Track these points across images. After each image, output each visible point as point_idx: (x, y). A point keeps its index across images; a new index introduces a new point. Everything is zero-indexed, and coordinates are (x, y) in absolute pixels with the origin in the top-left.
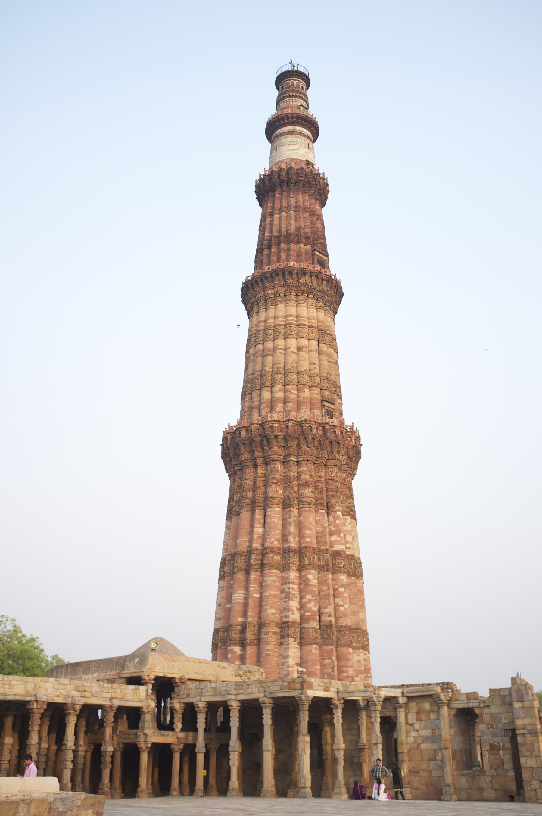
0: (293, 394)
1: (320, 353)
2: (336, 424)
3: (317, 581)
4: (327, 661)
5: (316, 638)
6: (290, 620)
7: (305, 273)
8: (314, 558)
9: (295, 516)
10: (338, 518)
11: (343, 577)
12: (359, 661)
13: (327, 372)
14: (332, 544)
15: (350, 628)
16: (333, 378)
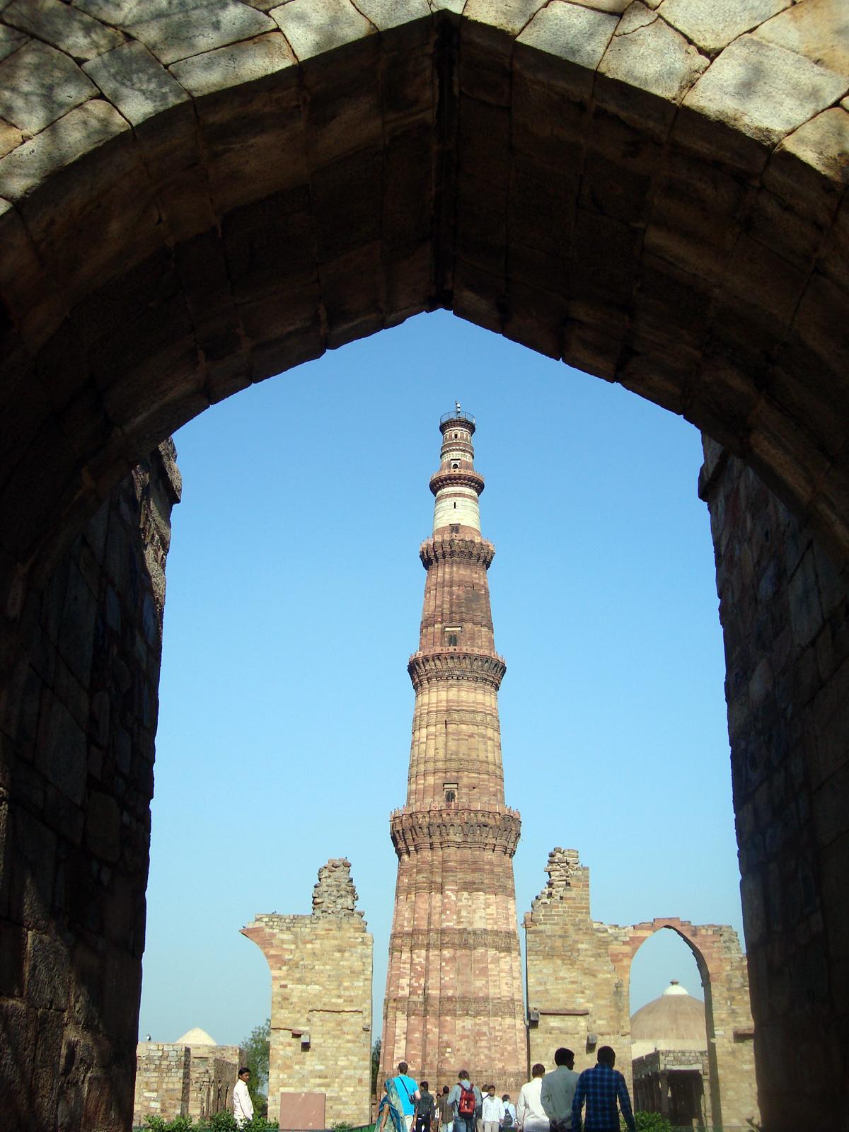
0: (421, 784)
1: (447, 734)
2: (443, 808)
3: (422, 960)
4: (425, 1030)
5: (415, 1010)
6: (400, 995)
7: (428, 661)
8: (418, 939)
9: (412, 902)
10: (447, 897)
11: (447, 953)
12: (463, 1027)
13: (450, 752)
14: (442, 921)
15: (450, 999)
16: (461, 756)
